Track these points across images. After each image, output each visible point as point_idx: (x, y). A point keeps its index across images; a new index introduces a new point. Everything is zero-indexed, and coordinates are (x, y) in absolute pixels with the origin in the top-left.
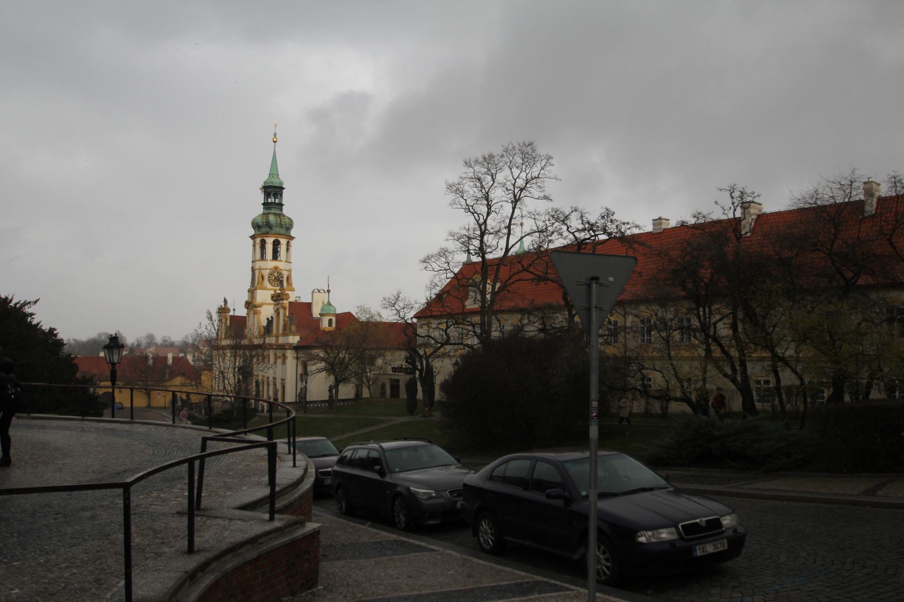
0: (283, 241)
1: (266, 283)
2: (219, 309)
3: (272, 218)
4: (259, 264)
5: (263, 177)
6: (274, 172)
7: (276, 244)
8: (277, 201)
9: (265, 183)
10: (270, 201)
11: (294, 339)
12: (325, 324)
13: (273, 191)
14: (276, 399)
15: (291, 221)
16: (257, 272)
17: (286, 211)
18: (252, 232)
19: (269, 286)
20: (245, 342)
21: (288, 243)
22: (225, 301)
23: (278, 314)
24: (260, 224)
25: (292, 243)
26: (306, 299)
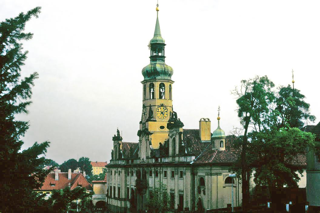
0: (167, 85)
3: (158, 67)
5: (150, 37)
6: (157, 32)
7: (162, 86)
8: (160, 54)
9: (152, 41)
10: (154, 54)
13: (157, 47)
18: (142, 78)
21: (170, 85)
22: (118, 132)
23: (174, 140)
25: (173, 85)
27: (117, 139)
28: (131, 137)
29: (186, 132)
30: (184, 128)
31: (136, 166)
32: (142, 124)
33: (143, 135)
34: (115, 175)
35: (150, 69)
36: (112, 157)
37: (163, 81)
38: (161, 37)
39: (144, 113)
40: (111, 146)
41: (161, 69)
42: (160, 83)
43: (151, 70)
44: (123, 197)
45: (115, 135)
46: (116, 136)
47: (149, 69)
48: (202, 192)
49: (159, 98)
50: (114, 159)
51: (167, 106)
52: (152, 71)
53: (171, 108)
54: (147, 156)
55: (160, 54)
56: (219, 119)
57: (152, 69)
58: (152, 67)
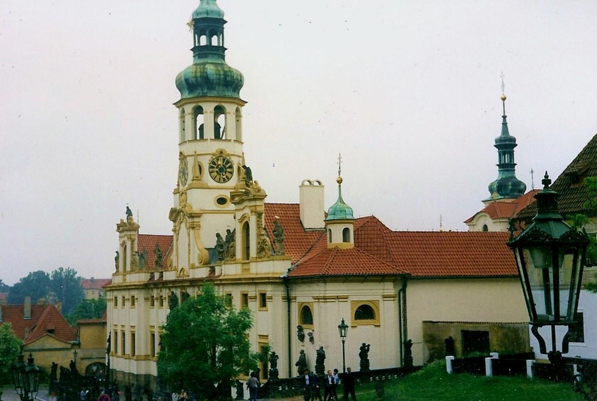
0: (230, 108)
1: (207, 178)
2: (119, 226)
3: (210, 69)
4: (189, 149)
8: (215, 41)
9: (196, 13)
11: (280, 267)
12: (337, 237)
14: (275, 373)
15: (241, 76)
16: (190, 161)
17: (232, 60)
18: (177, 96)
19: (212, 183)
20: (169, 276)
21: (237, 110)
22: (129, 212)
23: (246, 227)
24: (192, 80)
25: (243, 110)
26: (291, 197)
27: (127, 227)
28: (154, 222)
29: (272, 208)
30: (267, 200)
31: (164, 284)
32: (178, 195)
33: (180, 218)
34: (124, 305)
35: (194, 75)
36: (117, 267)
37: (222, 102)
38: (216, 5)
39: (183, 173)
40: (113, 242)
41: (216, 74)
42: (217, 104)
43: (196, 77)
44: (143, 353)
45: (122, 221)
46: (125, 221)
47: (190, 75)
48: (307, 338)
49: (214, 138)
50: (121, 269)
51: (232, 155)
52: (197, 80)
53: (241, 159)
54: (191, 262)
55: (215, 41)
56: (340, 182)
57: (198, 74)
58: (198, 70)
